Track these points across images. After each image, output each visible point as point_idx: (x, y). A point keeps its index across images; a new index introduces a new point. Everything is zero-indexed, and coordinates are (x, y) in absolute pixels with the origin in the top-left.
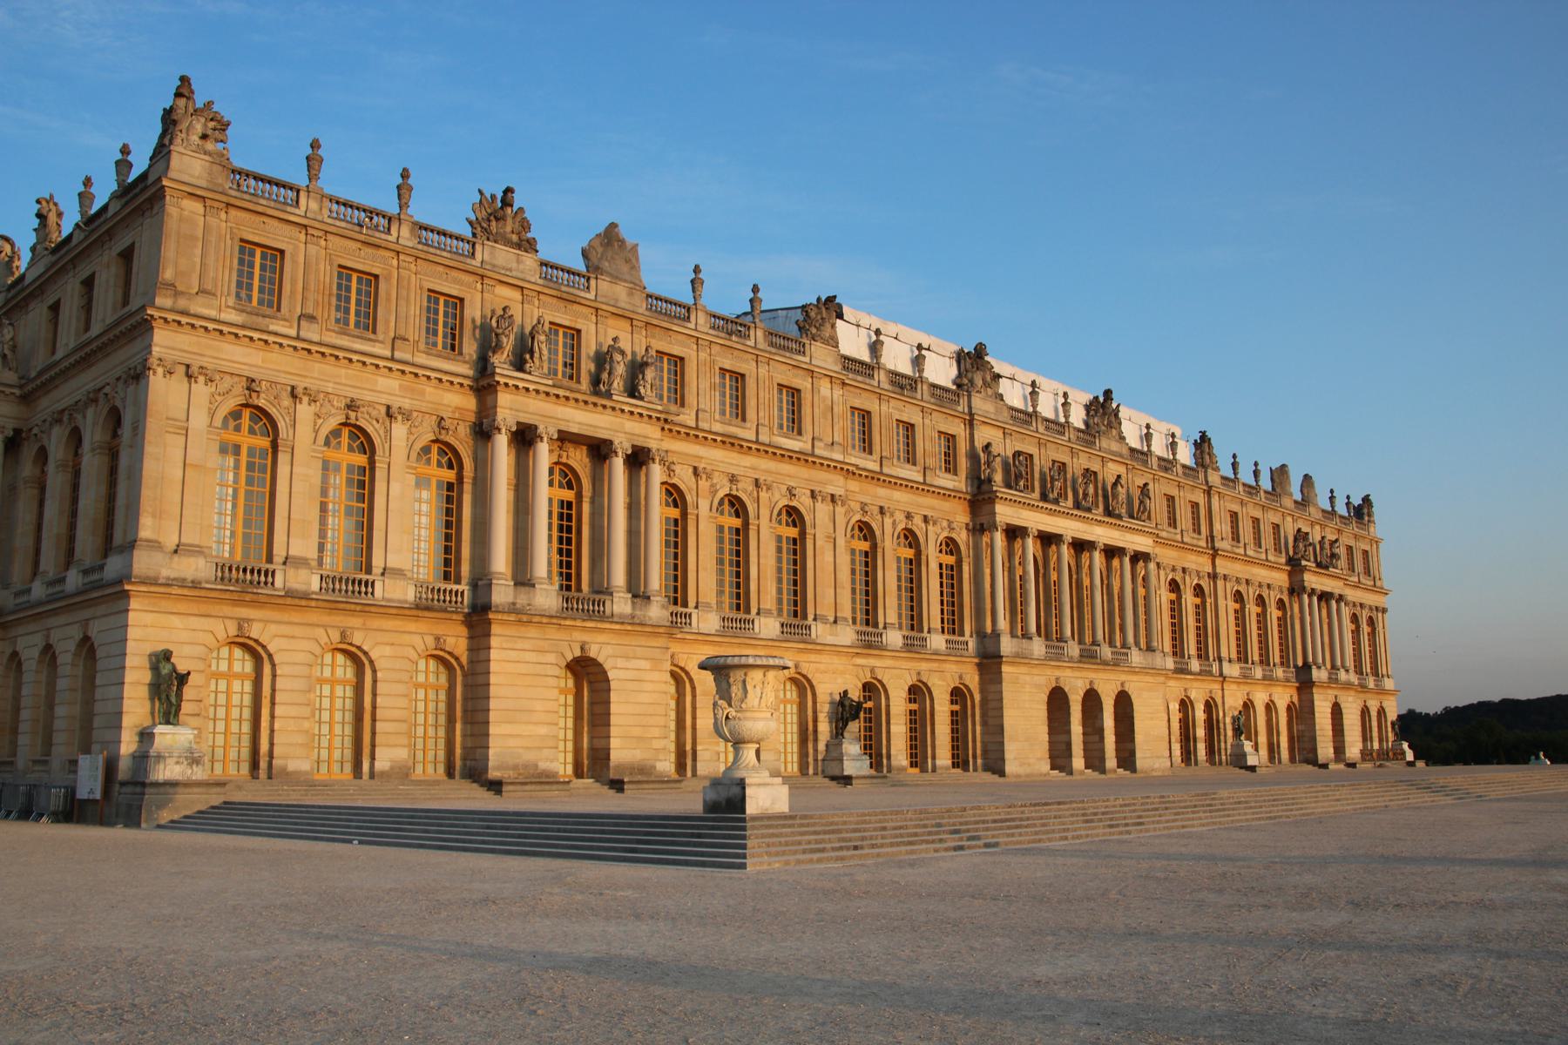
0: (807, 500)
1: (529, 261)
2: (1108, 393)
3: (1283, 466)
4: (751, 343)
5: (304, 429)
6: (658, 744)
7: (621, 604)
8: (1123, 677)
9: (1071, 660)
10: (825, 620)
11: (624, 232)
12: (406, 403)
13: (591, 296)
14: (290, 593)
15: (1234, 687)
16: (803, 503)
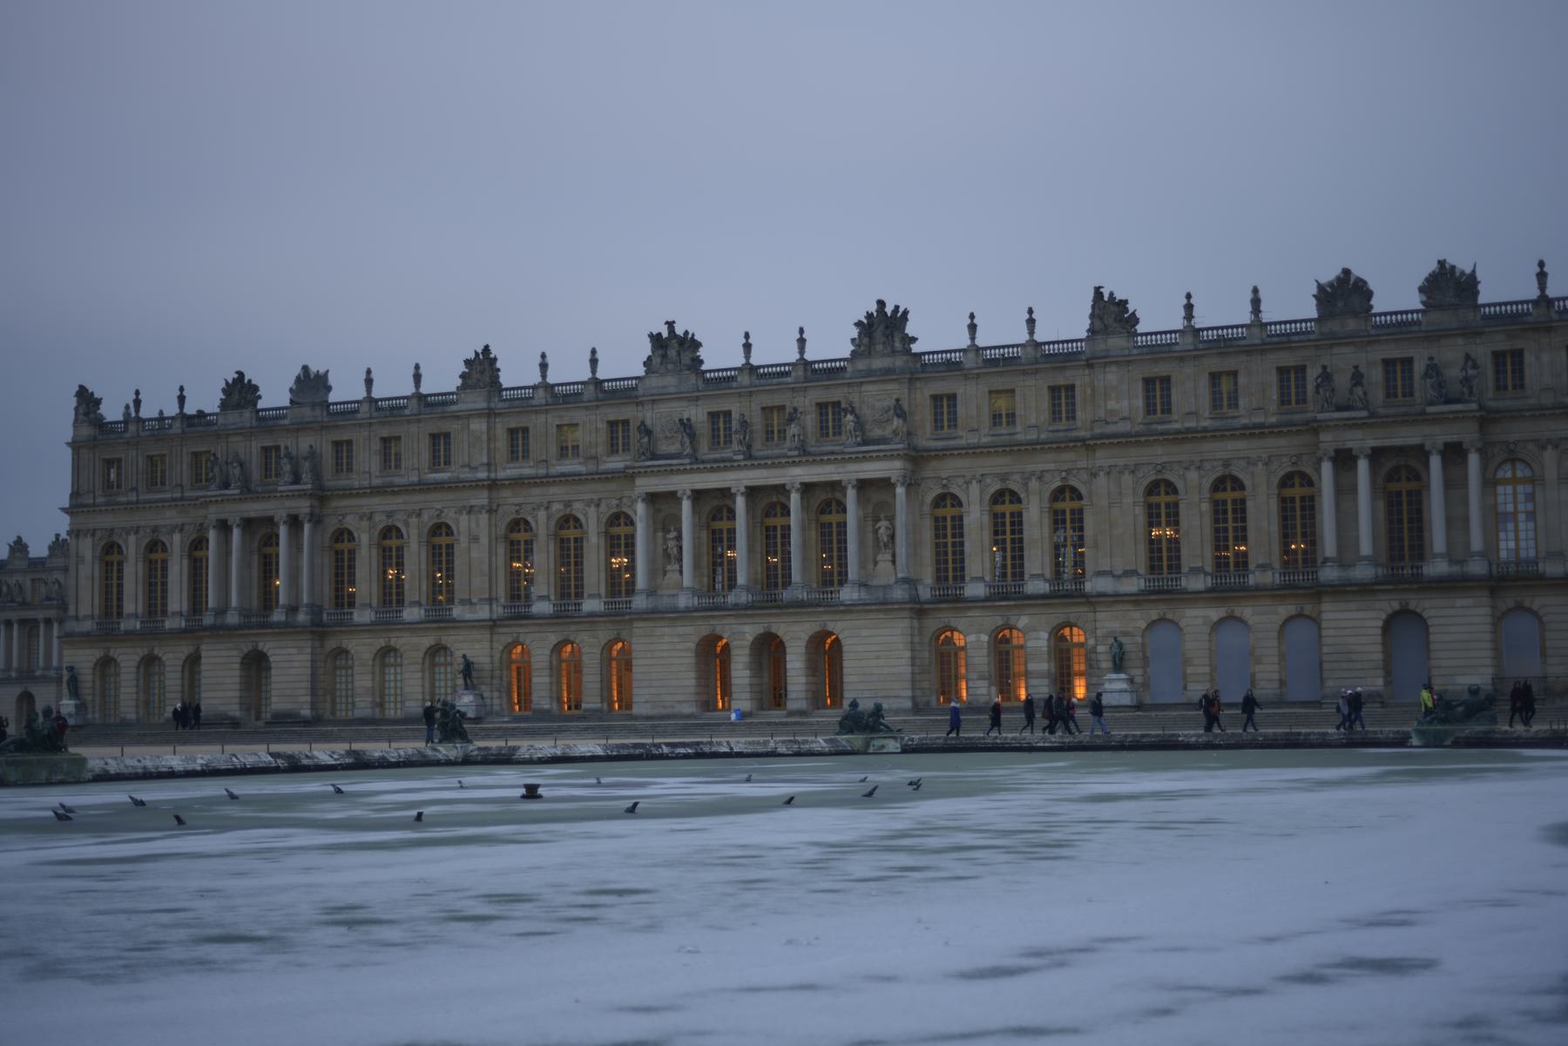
0: (452, 514)
1: (247, 414)
2: (881, 304)
3: (1347, 272)
4: (407, 412)
5: (132, 548)
6: (302, 699)
7: (278, 616)
8: (825, 618)
9: (736, 607)
10: (467, 602)
11: (313, 369)
12: (179, 521)
13: (286, 422)
14: (127, 633)
15: (1130, 607)
16: (449, 517)
